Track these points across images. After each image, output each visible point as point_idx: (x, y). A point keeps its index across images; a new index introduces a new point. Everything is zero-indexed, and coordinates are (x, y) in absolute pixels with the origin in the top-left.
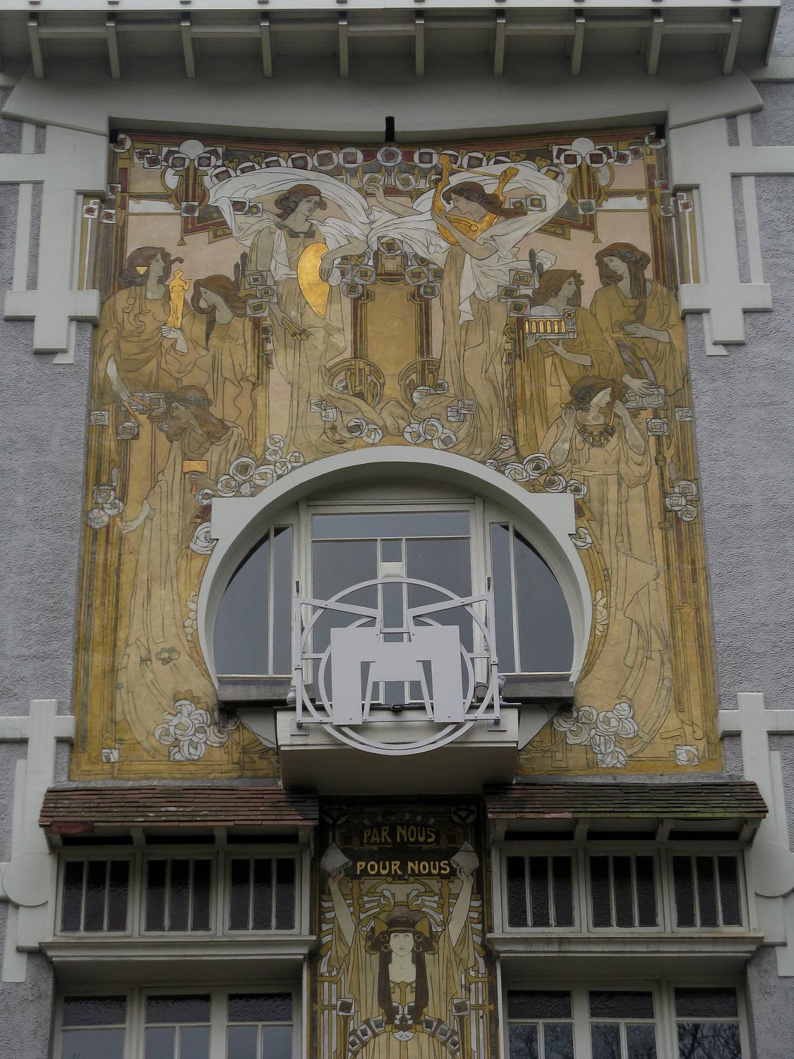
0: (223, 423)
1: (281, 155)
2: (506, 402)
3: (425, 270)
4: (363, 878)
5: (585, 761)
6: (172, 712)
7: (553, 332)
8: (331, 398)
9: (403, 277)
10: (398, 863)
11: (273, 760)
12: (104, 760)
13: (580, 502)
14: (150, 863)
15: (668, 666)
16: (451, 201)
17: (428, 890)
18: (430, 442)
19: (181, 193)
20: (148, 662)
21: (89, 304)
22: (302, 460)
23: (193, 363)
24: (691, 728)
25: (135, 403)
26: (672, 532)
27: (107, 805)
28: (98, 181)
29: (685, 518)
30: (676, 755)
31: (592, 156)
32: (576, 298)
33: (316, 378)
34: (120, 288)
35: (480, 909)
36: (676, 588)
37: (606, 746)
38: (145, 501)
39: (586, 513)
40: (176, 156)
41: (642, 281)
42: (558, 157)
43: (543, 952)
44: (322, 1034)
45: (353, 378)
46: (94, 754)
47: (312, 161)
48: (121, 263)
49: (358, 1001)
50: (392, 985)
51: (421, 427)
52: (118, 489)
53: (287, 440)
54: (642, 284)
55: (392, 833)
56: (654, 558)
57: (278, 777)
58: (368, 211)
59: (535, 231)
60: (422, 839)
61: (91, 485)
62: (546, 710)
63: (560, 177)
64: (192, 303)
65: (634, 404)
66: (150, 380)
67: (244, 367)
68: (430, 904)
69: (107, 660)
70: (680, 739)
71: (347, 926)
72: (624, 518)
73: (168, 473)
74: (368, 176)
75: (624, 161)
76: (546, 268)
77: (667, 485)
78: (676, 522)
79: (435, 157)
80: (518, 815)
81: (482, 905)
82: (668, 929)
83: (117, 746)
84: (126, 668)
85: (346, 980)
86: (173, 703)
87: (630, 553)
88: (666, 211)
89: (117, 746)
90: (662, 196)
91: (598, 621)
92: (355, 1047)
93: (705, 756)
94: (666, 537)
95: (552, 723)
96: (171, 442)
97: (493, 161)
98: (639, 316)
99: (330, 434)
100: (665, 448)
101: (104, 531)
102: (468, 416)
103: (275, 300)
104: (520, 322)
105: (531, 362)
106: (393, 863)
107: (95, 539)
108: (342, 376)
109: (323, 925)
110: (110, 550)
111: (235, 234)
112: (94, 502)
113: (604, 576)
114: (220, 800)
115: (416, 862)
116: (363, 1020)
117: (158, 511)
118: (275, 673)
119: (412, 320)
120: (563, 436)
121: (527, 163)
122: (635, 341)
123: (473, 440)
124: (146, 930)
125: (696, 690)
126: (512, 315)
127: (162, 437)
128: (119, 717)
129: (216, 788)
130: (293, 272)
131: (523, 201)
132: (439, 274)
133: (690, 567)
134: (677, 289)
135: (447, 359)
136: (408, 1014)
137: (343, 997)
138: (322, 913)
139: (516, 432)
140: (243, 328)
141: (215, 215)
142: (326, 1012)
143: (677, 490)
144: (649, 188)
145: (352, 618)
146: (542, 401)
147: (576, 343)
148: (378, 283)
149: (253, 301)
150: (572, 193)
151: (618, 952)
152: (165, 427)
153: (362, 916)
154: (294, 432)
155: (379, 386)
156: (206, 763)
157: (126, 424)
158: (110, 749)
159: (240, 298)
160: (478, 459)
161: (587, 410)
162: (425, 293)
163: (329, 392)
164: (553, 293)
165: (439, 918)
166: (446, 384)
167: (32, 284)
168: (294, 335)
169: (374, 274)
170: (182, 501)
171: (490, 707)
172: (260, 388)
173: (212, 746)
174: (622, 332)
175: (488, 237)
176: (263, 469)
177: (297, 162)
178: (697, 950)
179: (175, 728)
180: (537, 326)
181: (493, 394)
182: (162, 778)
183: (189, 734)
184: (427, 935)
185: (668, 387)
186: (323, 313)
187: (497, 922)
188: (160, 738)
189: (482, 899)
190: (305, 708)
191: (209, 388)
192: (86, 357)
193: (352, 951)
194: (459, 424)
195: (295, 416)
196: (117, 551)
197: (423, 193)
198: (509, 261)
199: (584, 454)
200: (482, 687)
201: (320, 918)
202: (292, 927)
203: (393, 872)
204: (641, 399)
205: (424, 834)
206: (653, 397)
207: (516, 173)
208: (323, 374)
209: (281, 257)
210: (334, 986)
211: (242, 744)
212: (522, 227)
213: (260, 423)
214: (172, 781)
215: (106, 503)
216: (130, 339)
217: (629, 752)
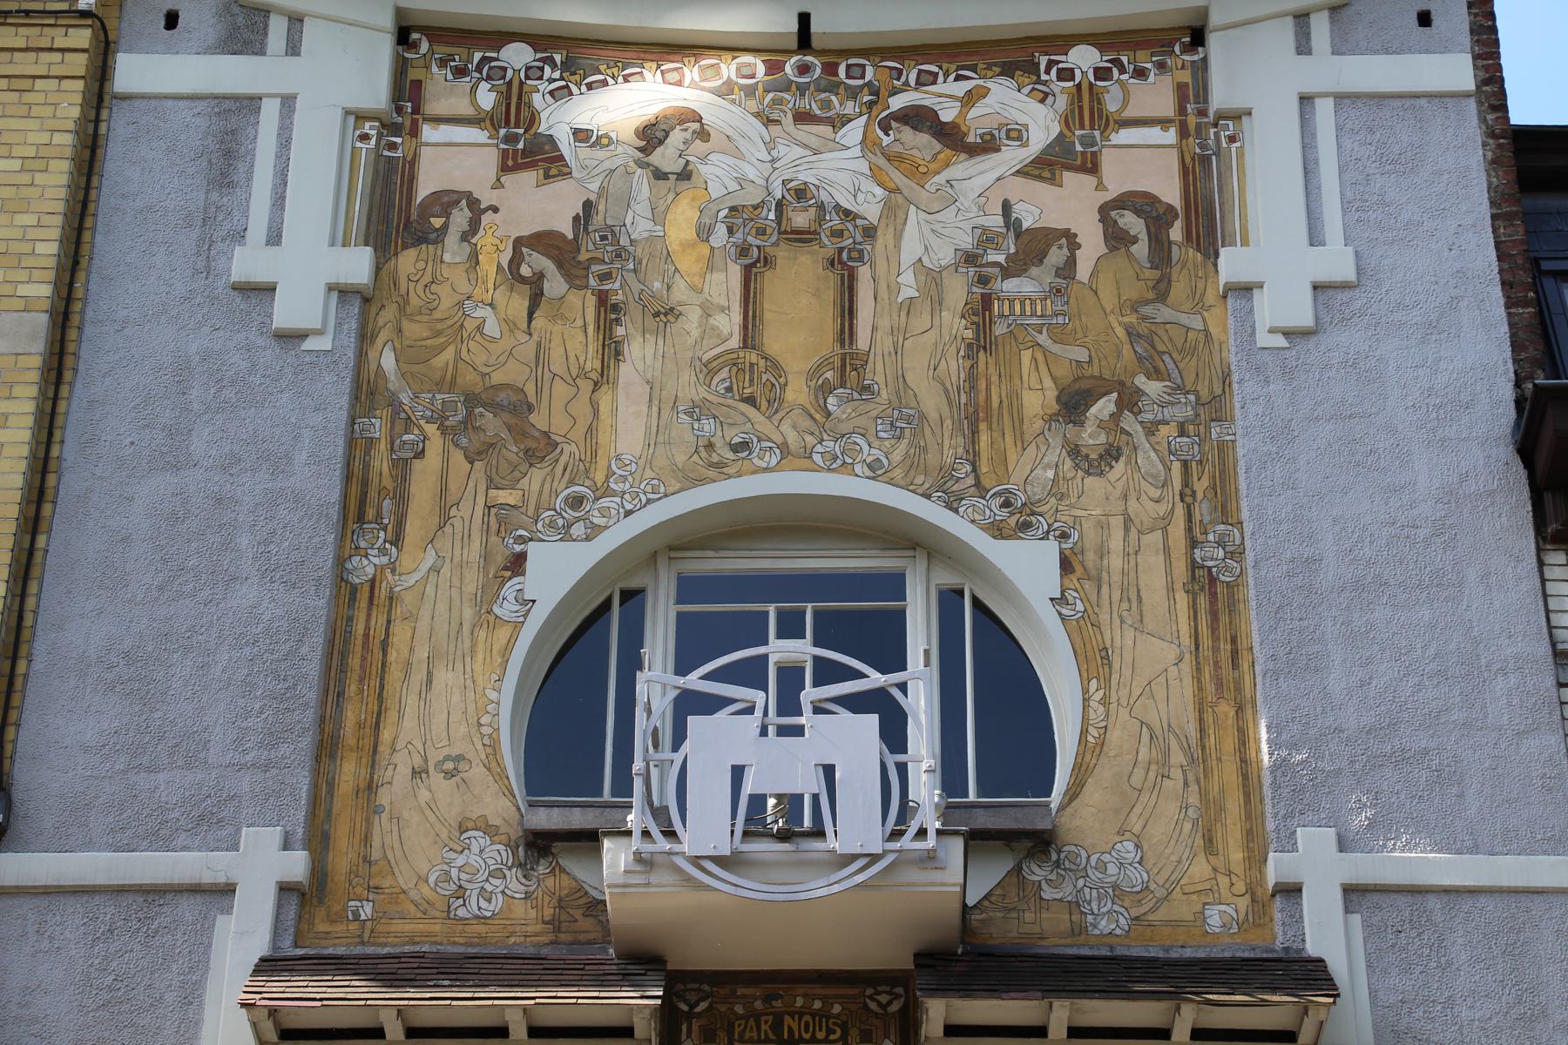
0: (549, 437)
2: (962, 412)
3: (851, 228)
5: (1069, 925)
6: (456, 847)
8: (707, 404)
9: (818, 237)
12: (350, 917)
13: (1067, 553)
15: (1194, 787)
16: (891, 132)
18: (850, 467)
19: (499, 116)
20: (424, 775)
21: (357, 265)
22: (662, 489)
23: (507, 353)
24: (1227, 880)
25: (420, 408)
26: (1202, 597)
28: (376, 93)
29: (1222, 578)
31: (1096, 70)
33: (687, 376)
34: (405, 247)
36: (1207, 675)
38: (430, 546)
39: (1076, 568)
40: (493, 64)
41: (1166, 245)
42: (1048, 72)
45: (741, 377)
46: (336, 908)
51: (837, 446)
52: (390, 527)
53: (642, 463)
54: (1166, 245)
56: (1175, 634)
58: (770, 145)
60: (820, 1035)
61: (350, 522)
63: (1050, 99)
64: (510, 269)
65: (1151, 417)
69: (363, 772)
70: (1209, 894)
72: (1132, 574)
74: (771, 95)
75: (1144, 78)
76: (1025, 225)
77: (1197, 531)
79: (870, 73)
86: (458, 834)
87: (1139, 626)
88: (1203, 147)
89: (371, 898)
90: (1199, 126)
91: (1091, 722)
94: (1194, 604)
96: (472, 463)
97: (952, 77)
98: (1161, 291)
99: (704, 454)
100: (1195, 478)
101: (367, 588)
102: (907, 432)
103: (631, 266)
104: (987, 301)
105: (1001, 355)
108: (724, 373)
110: (374, 614)
112: (353, 546)
113: (1102, 658)
114: (519, 972)
117: (448, 560)
118: (613, 795)
119: (830, 294)
120: (1046, 460)
121: (1002, 80)
123: (913, 464)
125: (1235, 824)
126: (975, 289)
127: (458, 457)
130: (659, 228)
132: (870, 232)
133: (1229, 647)
134: (1217, 255)
135: (879, 351)
139: (976, 454)
140: (583, 305)
141: (547, 147)
143: (1211, 537)
145: (724, 702)
148: (781, 244)
152: (464, 441)
154: (651, 451)
155: (778, 387)
156: (502, 922)
157: (406, 437)
158: (360, 901)
159: (580, 262)
160: (919, 491)
161: (1082, 424)
162: (850, 258)
163: (703, 394)
166: (876, 386)
167: (274, 238)
168: (657, 314)
169: (776, 232)
170: (484, 545)
171: (922, 833)
172: (604, 388)
174: (1135, 316)
175: (944, 182)
176: (605, 502)
177: (668, 76)
180: (1011, 307)
181: (945, 401)
182: (436, 943)
183: (479, 880)
185: (1201, 393)
186: (700, 286)
188: (436, 885)
190: (646, 834)
191: (530, 389)
192: (350, 342)
194: (893, 441)
195: (654, 429)
196: (385, 616)
197: (850, 120)
198: (972, 215)
199: (1075, 486)
204: (1160, 409)
205: (824, 1028)
206: (1179, 405)
207: (983, 93)
208: (698, 370)
209: (641, 208)
211: (557, 894)
213: (603, 437)
214: (449, 948)
216: (418, 318)
217: (1135, 912)
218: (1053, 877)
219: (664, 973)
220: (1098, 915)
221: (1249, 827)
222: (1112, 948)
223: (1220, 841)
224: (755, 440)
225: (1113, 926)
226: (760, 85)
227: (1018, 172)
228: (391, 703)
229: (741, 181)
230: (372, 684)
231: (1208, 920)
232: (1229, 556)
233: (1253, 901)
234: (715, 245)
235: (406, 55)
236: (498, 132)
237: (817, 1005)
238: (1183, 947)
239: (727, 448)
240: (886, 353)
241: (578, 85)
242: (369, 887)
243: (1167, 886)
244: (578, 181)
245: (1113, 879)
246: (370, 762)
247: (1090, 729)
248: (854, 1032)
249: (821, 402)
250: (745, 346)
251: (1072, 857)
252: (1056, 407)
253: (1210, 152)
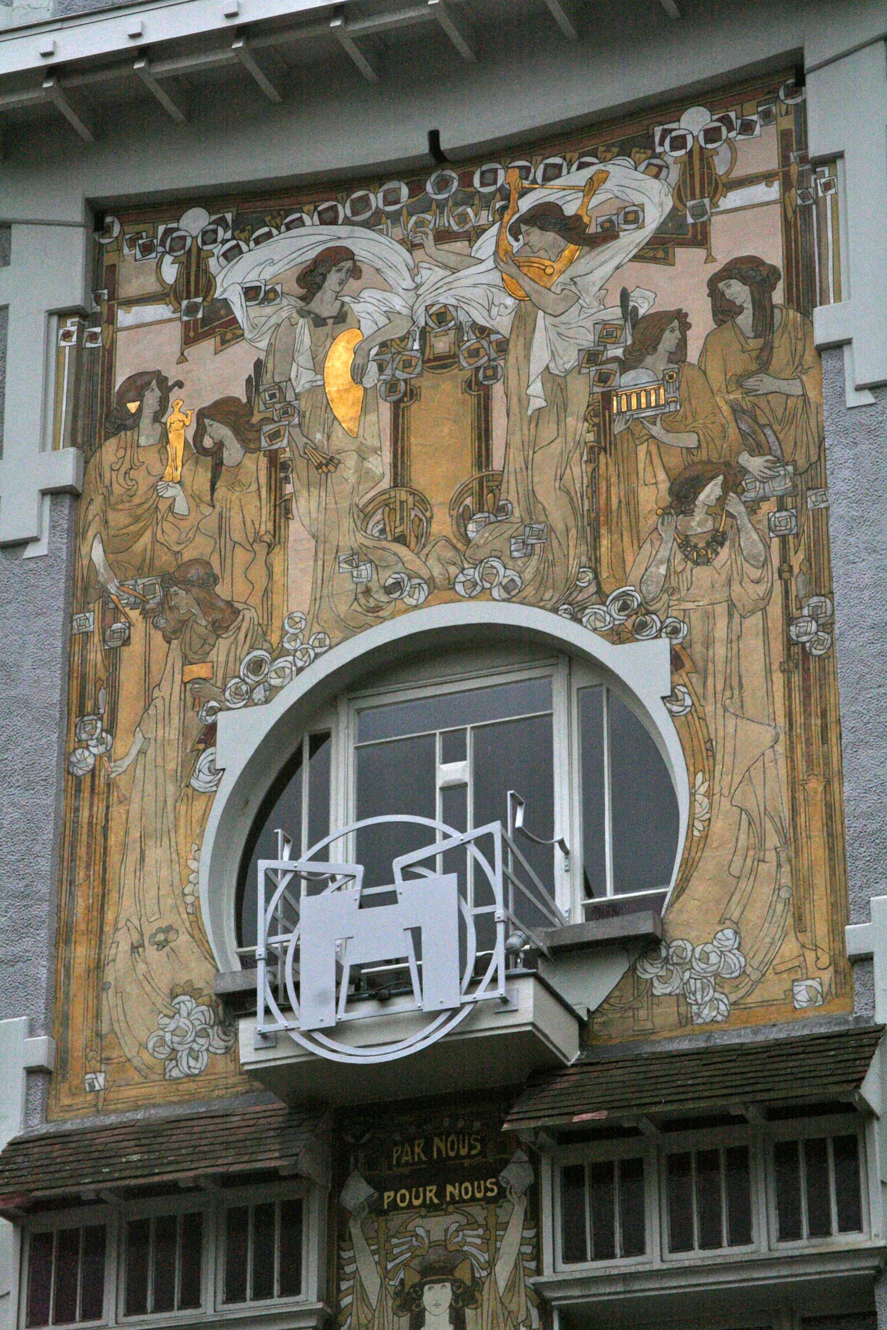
0: (232, 606)
1: (306, 208)
7: (649, 406)
12: (88, 1089)
13: (678, 648)
15: (786, 868)
16: (521, 237)
22: (327, 642)
25: (126, 596)
29: (814, 652)
30: (793, 997)
31: (707, 132)
32: (679, 354)
33: (347, 523)
34: (107, 438)
36: (799, 755)
40: (175, 235)
42: (661, 144)
46: (76, 1082)
47: (345, 210)
48: (108, 399)
53: (310, 617)
54: (769, 312)
55: (427, 1149)
56: (772, 717)
58: (414, 271)
59: (630, 260)
60: (463, 1152)
61: (73, 715)
62: (627, 951)
65: (752, 495)
66: (144, 560)
67: (257, 523)
68: (473, 1237)
69: (92, 953)
70: (798, 971)
71: (372, 1281)
72: (735, 663)
73: (166, 685)
74: (414, 219)
76: (642, 312)
78: (803, 660)
83: (103, 1068)
84: (114, 960)
88: (804, 197)
89: (103, 1069)
90: (801, 174)
94: (789, 682)
95: (635, 969)
96: (169, 642)
98: (764, 364)
99: (362, 601)
100: (792, 552)
101: (88, 778)
102: (537, 547)
103: (296, 421)
104: (607, 398)
105: (619, 452)
106: (428, 1188)
107: (78, 790)
108: (378, 517)
110: (96, 801)
111: (247, 335)
113: (707, 750)
117: (152, 741)
119: (468, 420)
120: (658, 557)
121: (621, 160)
122: (756, 401)
123: (542, 580)
124: (125, 1315)
127: (157, 637)
128: (105, 1028)
130: (319, 377)
131: (614, 218)
132: (503, 347)
135: (512, 469)
138: (340, 1267)
139: (598, 560)
143: (805, 612)
144: (783, 166)
146: (632, 510)
147: (678, 418)
148: (426, 374)
149: (271, 427)
150: (679, 196)
153: (390, 1266)
158: (95, 1073)
159: (253, 425)
160: (548, 606)
162: (486, 377)
164: (650, 349)
165: (483, 1257)
168: (319, 466)
171: (494, 980)
172: (277, 550)
176: (281, 662)
177: (325, 216)
181: (570, 512)
184: (468, 1283)
187: (547, 1258)
195: (319, 582)
197: (484, 231)
201: (338, 1273)
206: (778, 479)
212: (611, 258)
213: (277, 599)
215: (92, 739)
216: (119, 507)
217: (733, 998)
218: (663, 973)
223: (808, 917)
224: (406, 579)
225: (714, 1014)
226: (405, 212)
227: (637, 258)
228: (112, 885)
229: (389, 315)
230: (97, 868)
232: (821, 629)
233: (836, 972)
234: (368, 386)
235: (103, 241)
236: (180, 304)
237: (461, 1124)
239: (382, 591)
240: (518, 470)
241: (247, 242)
244: (250, 340)
245: (715, 968)
247: (696, 823)
249: (462, 530)
250: (396, 486)
252: (669, 499)
253: (811, 201)
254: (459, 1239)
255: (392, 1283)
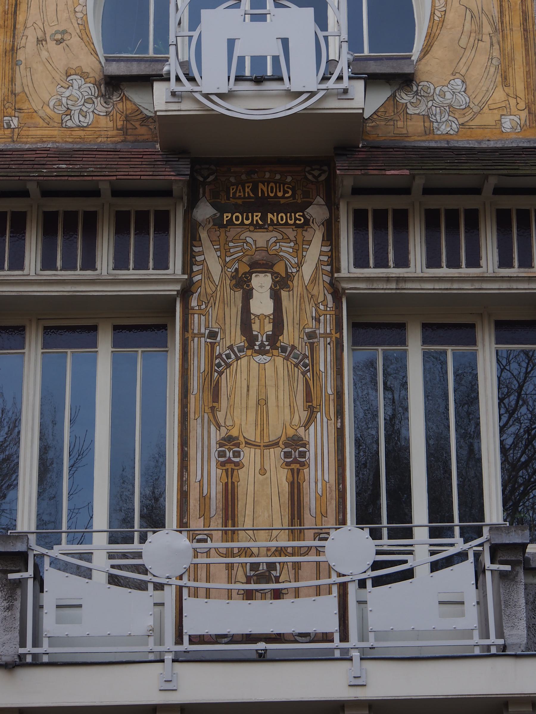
4: (229, 227)
6: (64, 85)
10: (260, 214)
11: (152, 127)
12: (5, 126)
14: (45, 213)
15: (496, 46)
17: (285, 237)
20: (44, 43)
27: (7, 163)
35: (330, 254)
37: (441, 116)
43: (382, 289)
44: (192, 357)
49: (225, 333)
50: (253, 317)
55: (255, 189)
57: (156, 142)
60: (280, 194)
62: (390, 85)
68: (287, 248)
69: (8, 40)
70: (505, 110)
80: (363, 172)
81: (331, 250)
82: (490, 270)
83: (17, 114)
85: (213, 313)
86: (65, 78)
89: (17, 114)
91: (436, 8)
92: (220, 369)
93: (526, 124)
106: (255, 214)
109: (194, 267)
114: (105, 159)
115: (275, 214)
116: (227, 346)
124: (41, 270)
125: (520, 68)
128: (18, 89)
129: (103, 150)
136: (266, 341)
137: (210, 327)
142: (196, 339)
151: (447, 289)
153: (228, 259)
158: (11, 117)
165: (294, 261)
171: (340, 78)
173: (99, 115)
178: (515, 287)
179: (67, 99)
182: (55, 142)
184: (284, 275)
187: (344, 264)
188: (54, 107)
189: (331, 245)
190: (178, 79)
193: (218, 288)
200: (332, 63)
202: (167, 268)
203: (255, 222)
205: (282, 190)
210: (203, 318)
211: (125, 113)
214: (64, 145)
217: (461, 121)
218: (414, 100)
219: (189, 160)
220: (440, 123)
221: (528, 69)
222: (448, 142)
223: (511, 78)
225: (449, 129)
231: (503, 125)
233: (529, 113)
238: (489, 140)
242: (15, 109)
243: (480, 105)
245: (449, 101)
246: (12, 35)
247: (436, 12)
248: (299, 192)
251: (425, 89)
254: (277, 247)
255: (229, 270)
